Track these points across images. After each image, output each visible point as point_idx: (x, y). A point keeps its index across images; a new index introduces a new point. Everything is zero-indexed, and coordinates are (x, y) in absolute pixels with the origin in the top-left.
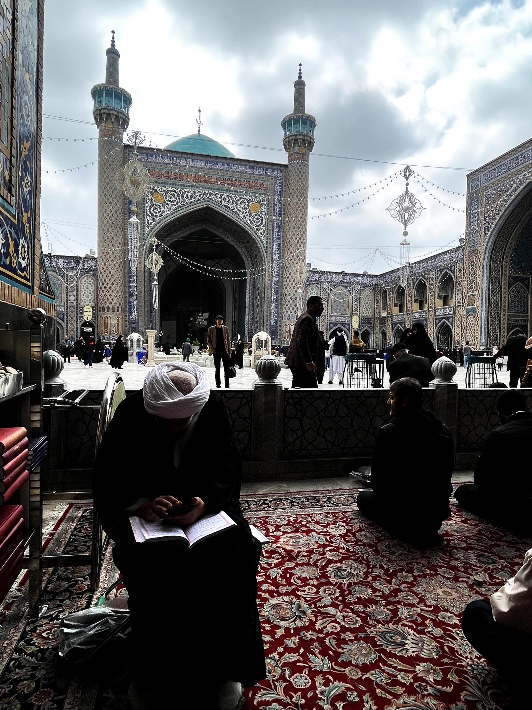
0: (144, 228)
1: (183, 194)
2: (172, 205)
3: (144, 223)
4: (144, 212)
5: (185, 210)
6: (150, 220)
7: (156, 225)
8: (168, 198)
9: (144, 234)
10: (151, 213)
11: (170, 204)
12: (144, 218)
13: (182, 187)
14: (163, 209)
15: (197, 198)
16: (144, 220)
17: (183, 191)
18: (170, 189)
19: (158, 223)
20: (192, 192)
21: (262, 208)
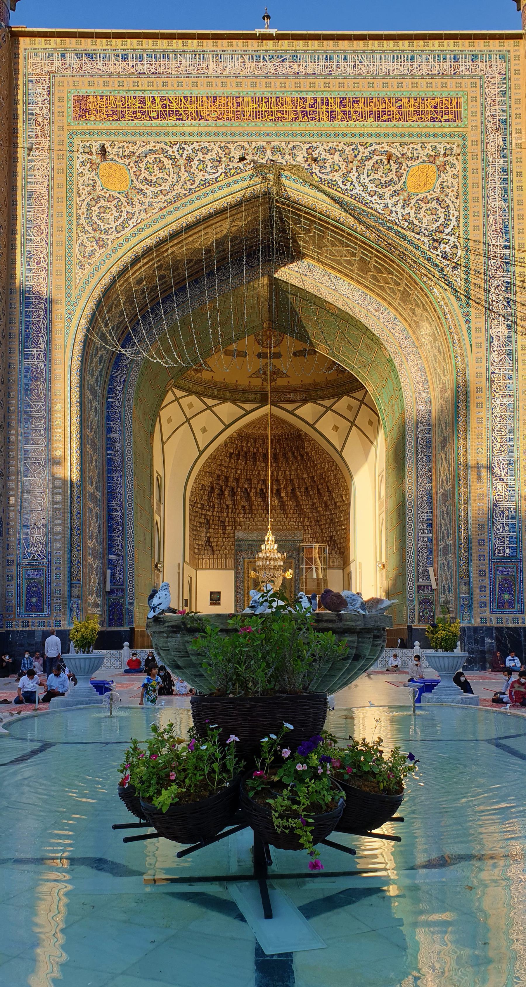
0: (70, 271)
1: (190, 159)
2: (156, 195)
3: (70, 255)
4: (70, 222)
5: (197, 204)
6: (88, 244)
7: (109, 256)
8: (145, 174)
9: (69, 287)
10: (92, 224)
11: (150, 191)
12: (70, 238)
13: (188, 139)
14: (129, 209)
15: (232, 165)
16: (70, 247)
17: (189, 149)
18: (150, 147)
19: (114, 250)
20: (216, 148)
21: (447, 177)
